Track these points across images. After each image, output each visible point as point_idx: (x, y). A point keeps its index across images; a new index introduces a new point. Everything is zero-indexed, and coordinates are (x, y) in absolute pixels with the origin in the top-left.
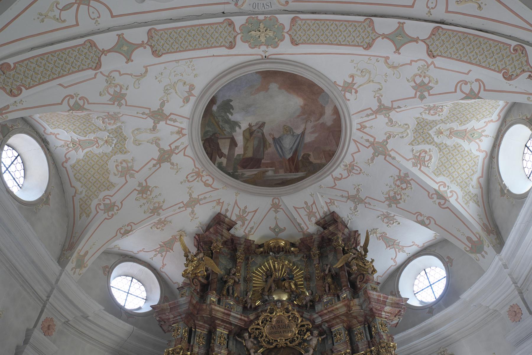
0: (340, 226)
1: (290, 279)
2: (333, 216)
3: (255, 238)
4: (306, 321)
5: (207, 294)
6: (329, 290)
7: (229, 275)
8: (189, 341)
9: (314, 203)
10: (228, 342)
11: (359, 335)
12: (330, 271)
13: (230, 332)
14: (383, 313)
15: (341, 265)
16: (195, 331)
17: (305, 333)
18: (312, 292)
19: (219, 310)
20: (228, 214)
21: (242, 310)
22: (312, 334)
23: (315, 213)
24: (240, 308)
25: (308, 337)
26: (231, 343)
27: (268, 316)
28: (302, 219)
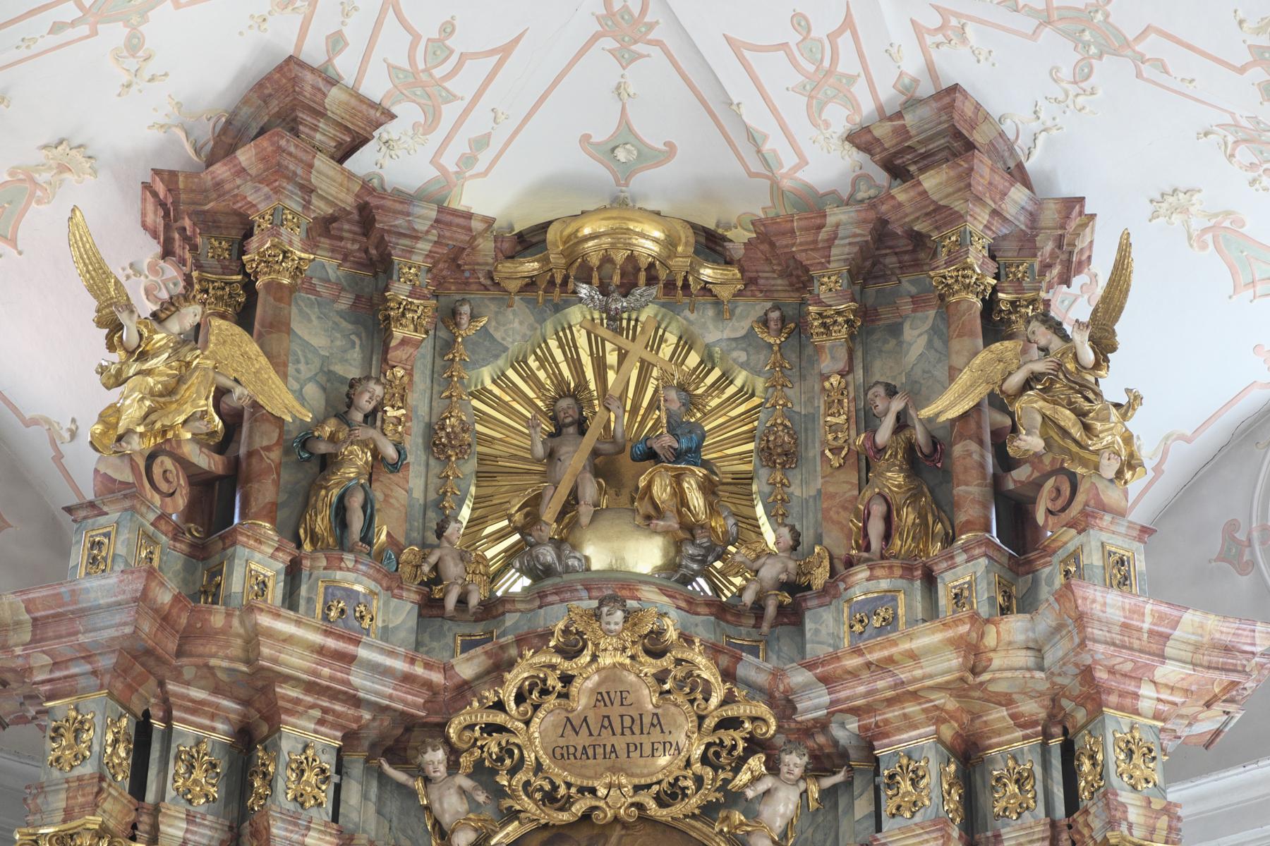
0: (984, 171)
1: (679, 456)
2: (951, 106)
3: (493, 196)
4: (749, 699)
5: (230, 541)
6: (887, 537)
7: (343, 418)
8: (138, 788)
9: (848, 23)
10: (338, 788)
11: (1013, 788)
12: (902, 423)
13: (350, 737)
14: (1147, 690)
15: (966, 405)
16: (168, 733)
17: (743, 760)
18: (796, 536)
19: (292, 641)
20: (345, 66)
21: (412, 622)
22: (773, 767)
23: (852, 79)
24: (400, 612)
25: (756, 779)
26: (352, 794)
27: (553, 667)
28: (774, 110)
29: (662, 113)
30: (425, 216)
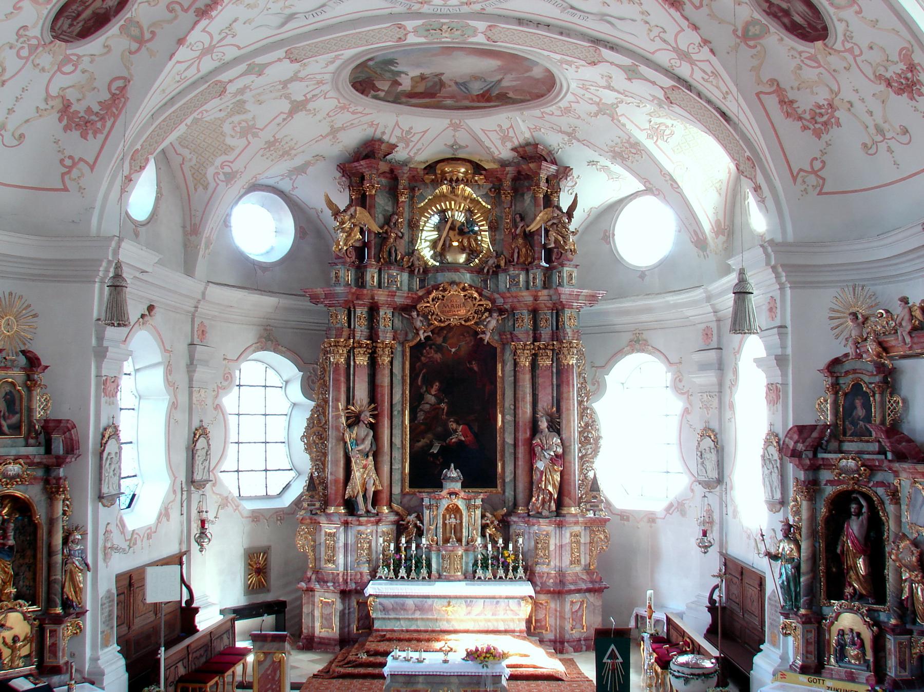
20: (386, 138)
29: (463, 138)
30: (406, 169)
